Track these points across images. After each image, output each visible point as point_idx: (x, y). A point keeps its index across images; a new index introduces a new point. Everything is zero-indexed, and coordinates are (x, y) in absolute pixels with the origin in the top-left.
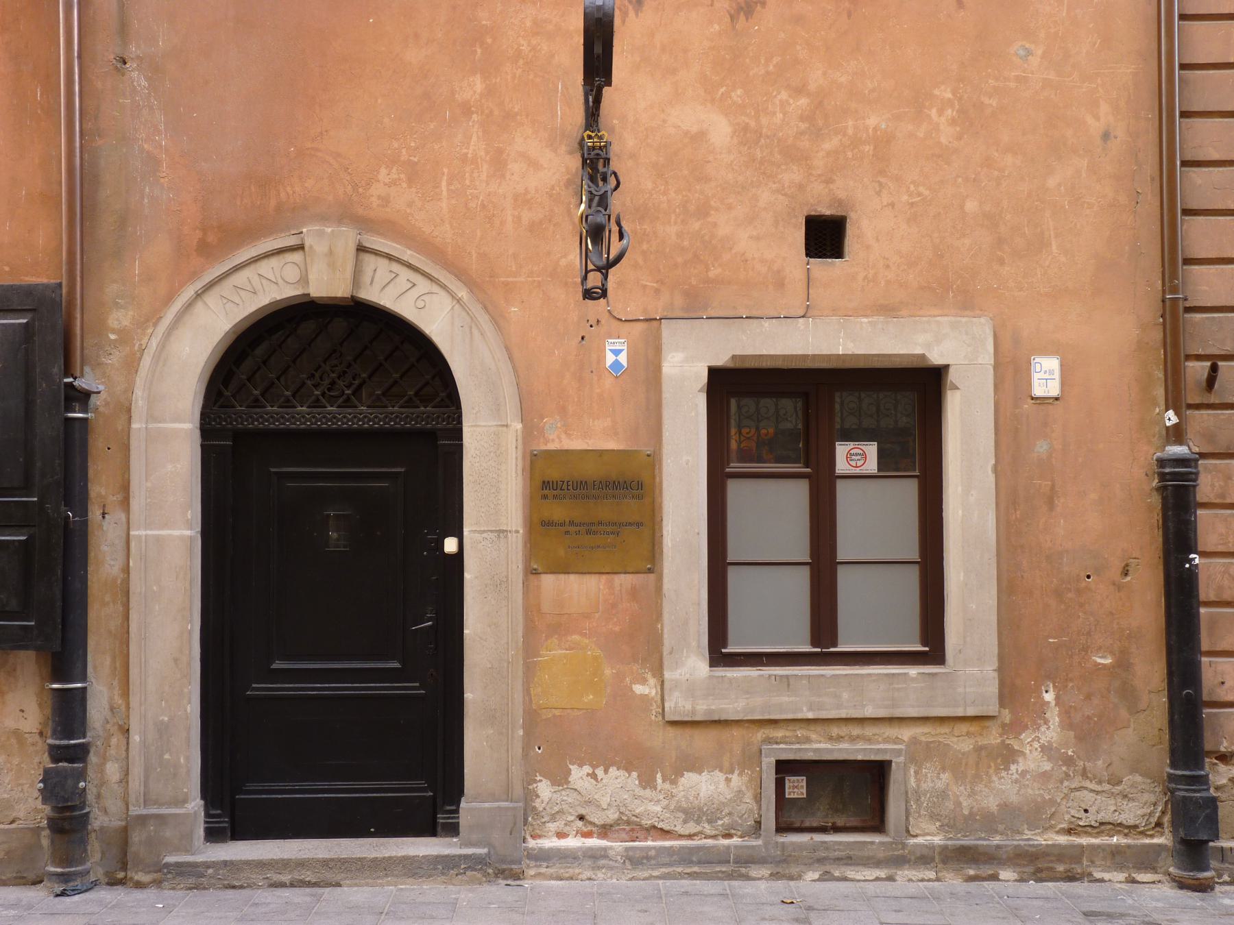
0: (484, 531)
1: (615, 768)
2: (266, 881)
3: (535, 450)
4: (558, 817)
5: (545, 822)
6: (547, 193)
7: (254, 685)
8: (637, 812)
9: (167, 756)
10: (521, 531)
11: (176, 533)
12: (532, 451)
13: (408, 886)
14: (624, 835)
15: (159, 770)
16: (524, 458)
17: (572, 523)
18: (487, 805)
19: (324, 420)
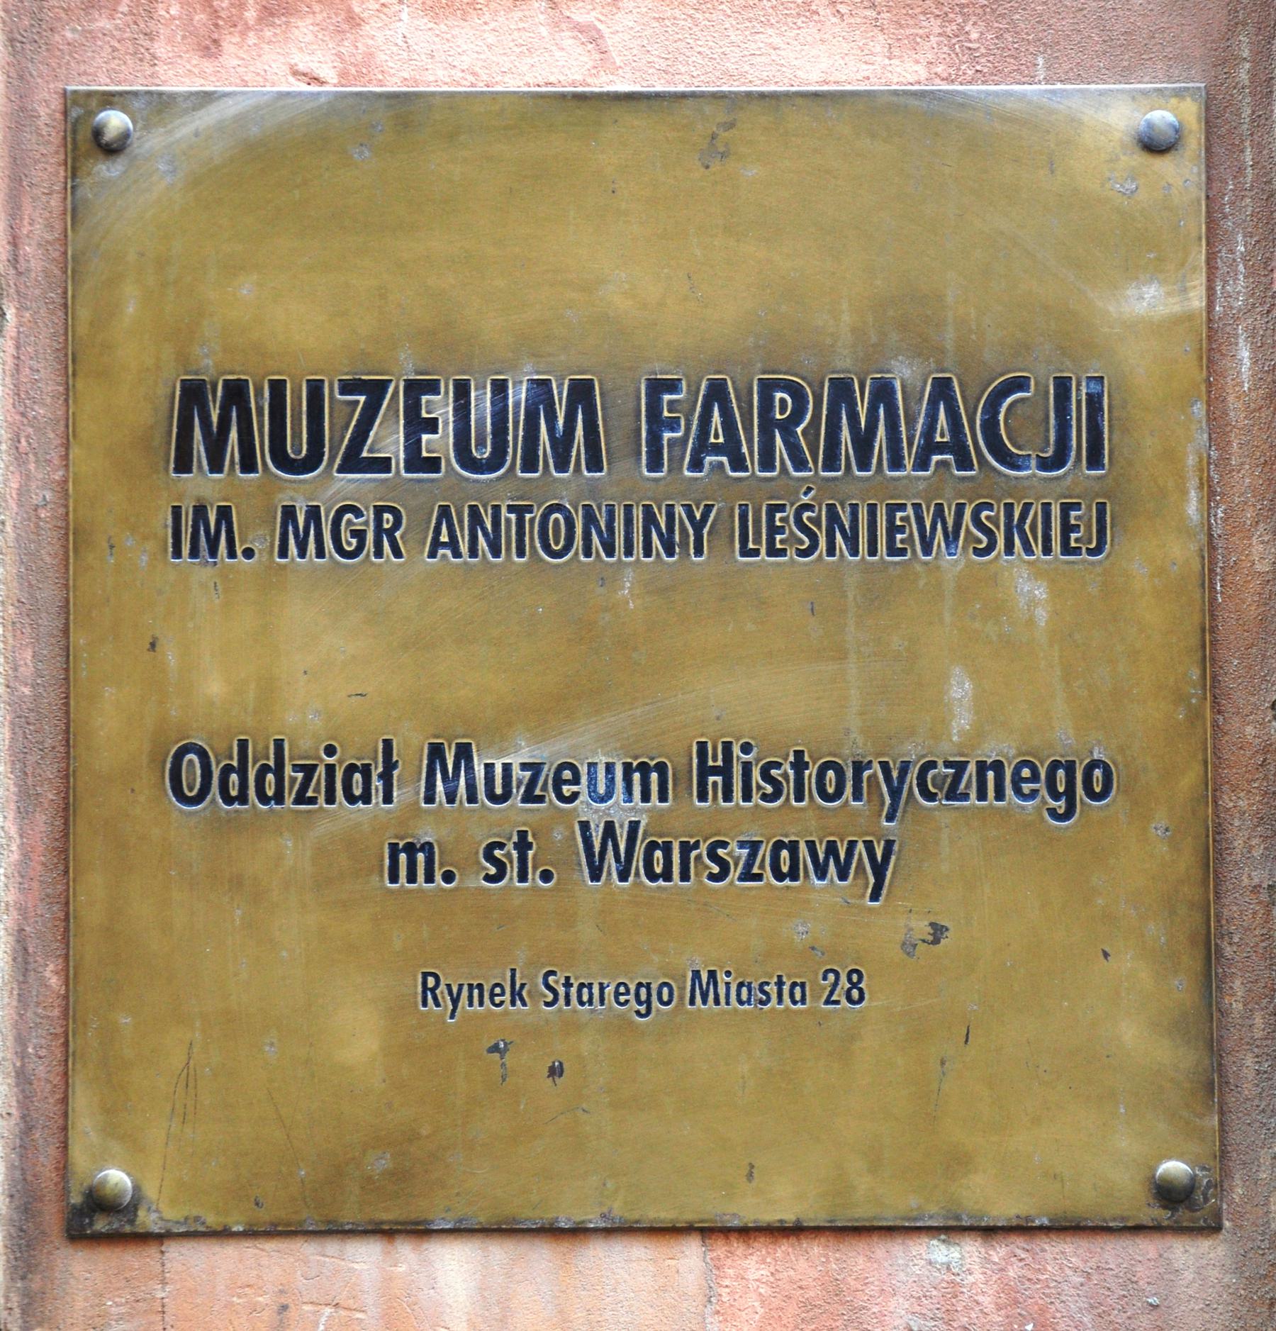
3: (109, 100)
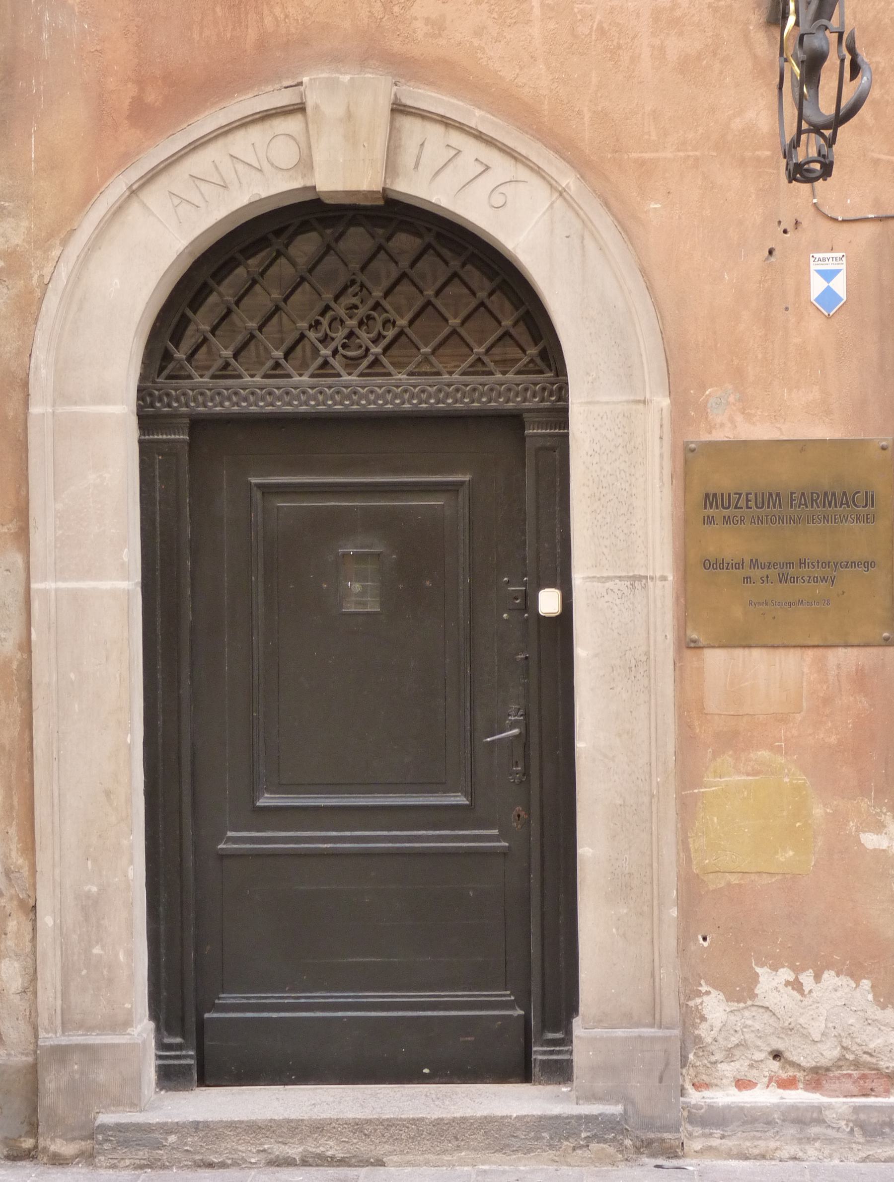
0: (608, 579)
1: (833, 973)
2: (263, 1155)
3: (692, 442)
4: (737, 1053)
5: (715, 1063)
6: (709, 5)
7: (229, 834)
8: (872, 1046)
9: (97, 950)
10: (671, 578)
11: (106, 585)
12: (686, 444)
13: (494, 1167)
14: (849, 1086)
15: (84, 972)
16: (673, 454)
17: (754, 563)
18: (620, 1033)
19: (337, 398)
